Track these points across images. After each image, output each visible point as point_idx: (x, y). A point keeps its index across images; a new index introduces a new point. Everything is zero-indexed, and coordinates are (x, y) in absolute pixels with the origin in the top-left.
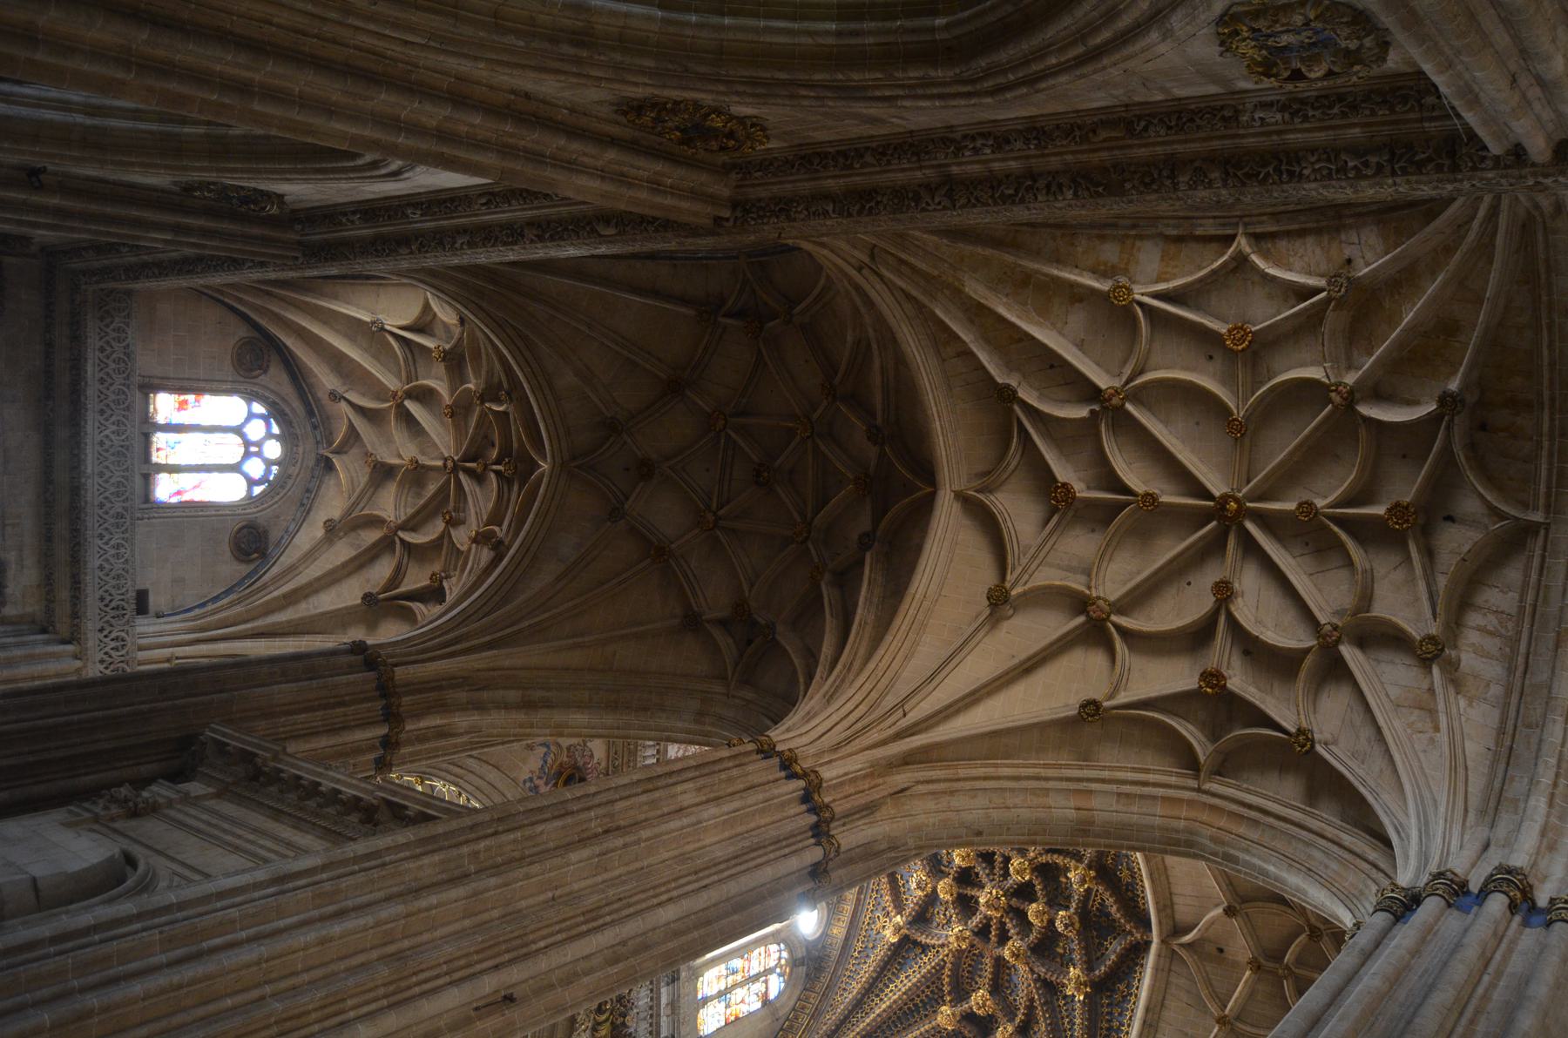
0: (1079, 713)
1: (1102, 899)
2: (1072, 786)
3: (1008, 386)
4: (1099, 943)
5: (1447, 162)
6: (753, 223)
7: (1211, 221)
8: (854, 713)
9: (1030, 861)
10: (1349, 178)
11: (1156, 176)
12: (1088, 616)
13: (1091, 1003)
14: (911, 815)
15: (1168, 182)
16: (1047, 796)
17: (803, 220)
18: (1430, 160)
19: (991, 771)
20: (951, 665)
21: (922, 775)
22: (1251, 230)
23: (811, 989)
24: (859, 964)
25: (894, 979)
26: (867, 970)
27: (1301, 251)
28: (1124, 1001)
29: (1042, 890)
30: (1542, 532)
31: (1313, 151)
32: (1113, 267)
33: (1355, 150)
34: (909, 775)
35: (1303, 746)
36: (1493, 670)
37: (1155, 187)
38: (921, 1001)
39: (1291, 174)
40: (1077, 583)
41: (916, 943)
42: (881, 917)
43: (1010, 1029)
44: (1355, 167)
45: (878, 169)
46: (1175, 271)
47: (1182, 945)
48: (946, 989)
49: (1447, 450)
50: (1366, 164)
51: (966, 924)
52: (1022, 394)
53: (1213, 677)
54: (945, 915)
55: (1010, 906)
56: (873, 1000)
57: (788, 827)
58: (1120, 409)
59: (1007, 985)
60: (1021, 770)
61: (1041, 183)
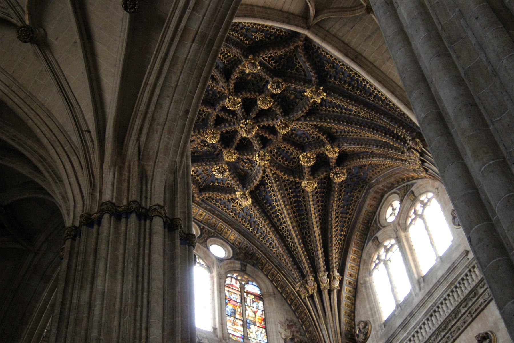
0: (130, 13)
1: (269, 58)
2: (177, 39)
4: (296, 70)
8: (75, 166)
9: (230, 94)
14: (158, 152)
19: (148, 88)
20: (66, 87)
21: (134, 136)
24: (258, 229)
25: (274, 210)
26: (264, 226)
28: (337, 69)
29: (251, 94)
34: (131, 143)
38: (294, 197)
41: (257, 187)
42: (234, 205)
43: (328, 147)
47: (315, 17)
48: (291, 179)
51: (256, 151)
55: (254, 118)
56: (283, 228)
57: (132, 234)
59: (302, 139)
60: (155, 68)
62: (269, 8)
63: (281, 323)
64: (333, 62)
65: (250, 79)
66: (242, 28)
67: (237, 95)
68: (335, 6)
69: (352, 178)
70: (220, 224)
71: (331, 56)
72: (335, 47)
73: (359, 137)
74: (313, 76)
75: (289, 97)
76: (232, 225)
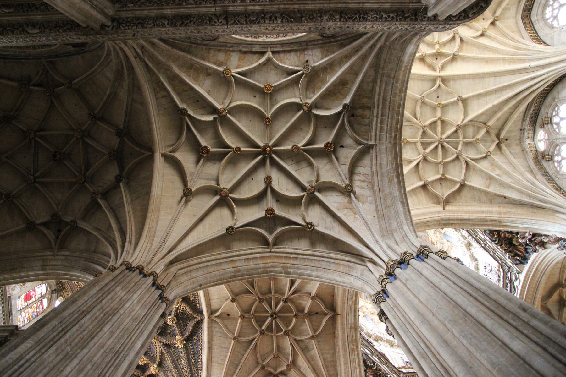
3: (184, 109)
5: (414, 18)
6: (123, 28)
7: (259, 46)
10: (382, 21)
11: (315, 16)
12: (221, 195)
13: (186, 347)
15: (319, 19)
16: (221, 265)
17: (150, 28)
18: (409, 16)
19: (199, 260)
22: (272, 49)
27: (289, 58)
30: (375, 147)
31: (372, 11)
32: (222, 62)
33: (385, 11)
35: (310, 228)
36: (367, 192)
37: (314, 20)
39: (364, 18)
40: (213, 183)
43: (156, 366)
44: (385, 17)
45: (194, 6)
46: (244, 64)
49: (343, 123)
50: (389, 16)
52: (190, 112)
53: (270, 211)
58: (225, 116)
59: (149, 350)
60: (209, 258)
61: (268, 16)
62: (209, 294)
64: (200, 340)
71: (201, 336)
72: (209, 335)
74: (187, 334)
75: (167, 330)
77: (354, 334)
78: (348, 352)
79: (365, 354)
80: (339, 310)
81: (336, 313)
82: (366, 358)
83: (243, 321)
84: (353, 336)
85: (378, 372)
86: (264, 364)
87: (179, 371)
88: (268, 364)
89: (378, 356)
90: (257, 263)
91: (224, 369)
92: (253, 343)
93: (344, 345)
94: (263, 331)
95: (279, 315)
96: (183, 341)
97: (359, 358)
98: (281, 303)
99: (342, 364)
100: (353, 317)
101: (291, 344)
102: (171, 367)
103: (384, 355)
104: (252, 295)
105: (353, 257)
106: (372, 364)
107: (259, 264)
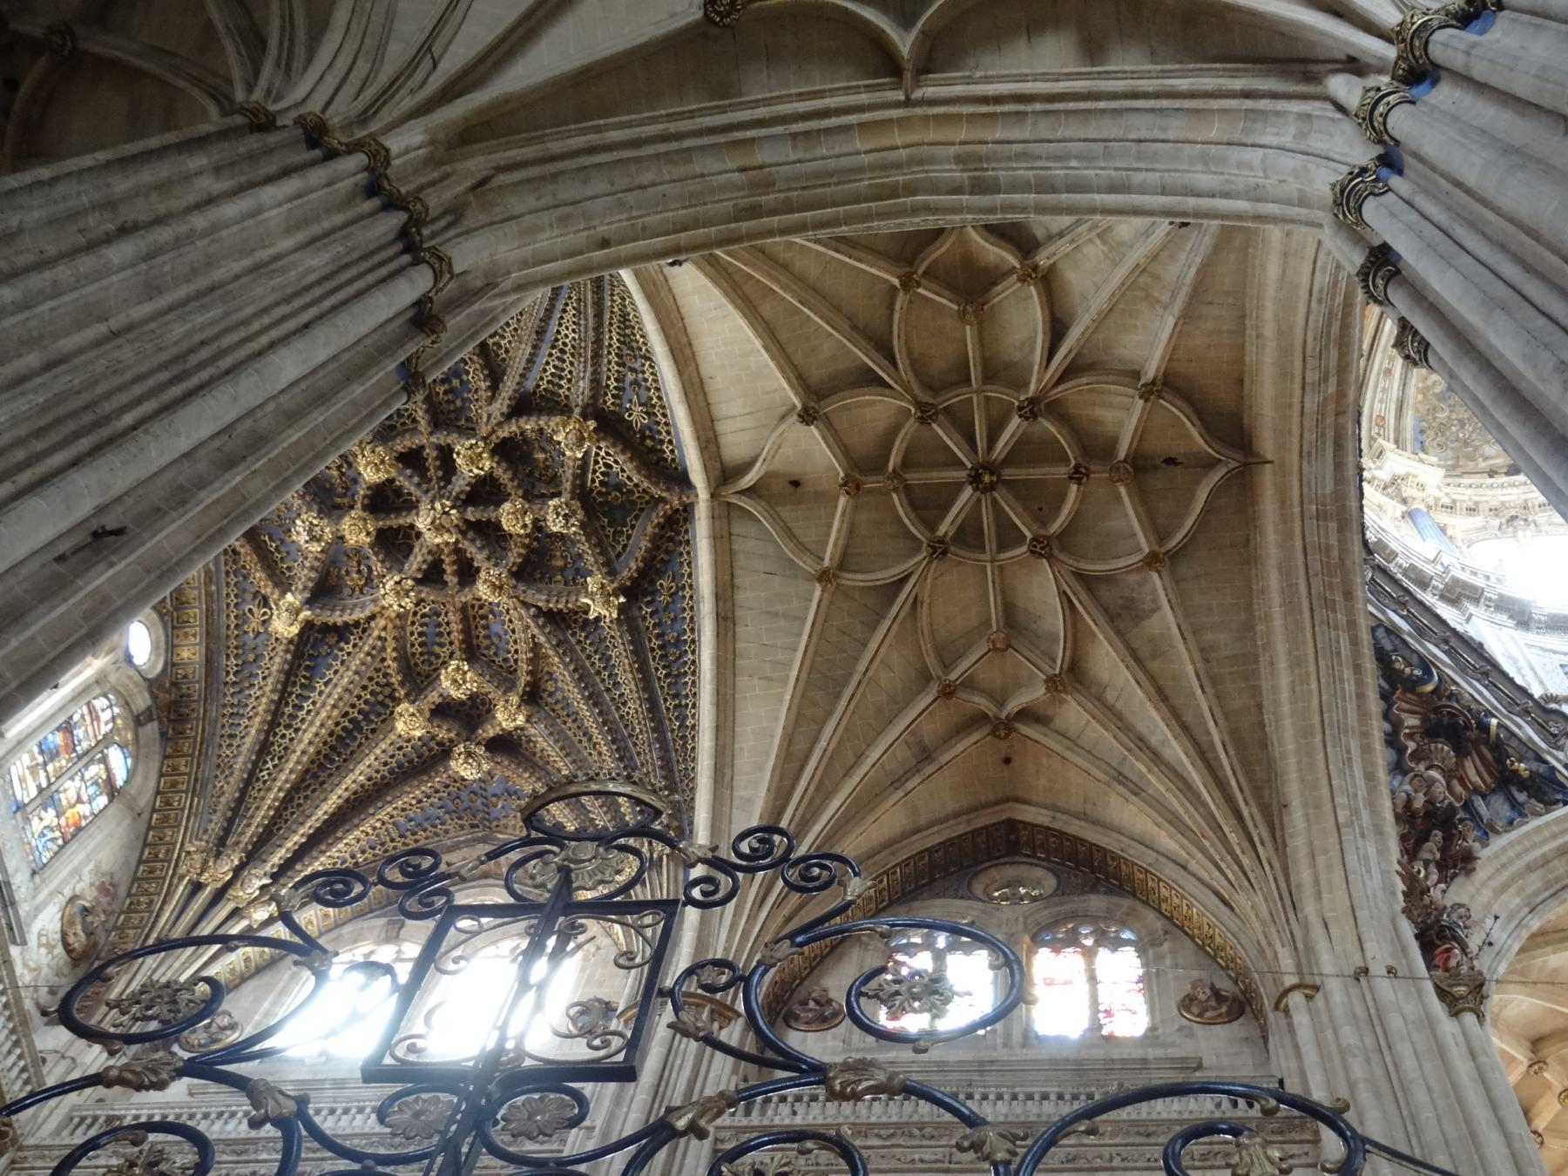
0: (706, 14)
1: (606, 465)
2: (721, 139)
8: (355, 72)
16: (690, 161)
19: (593, 138)
21: (501, 157)
23: (178, 753)
24: (241, 691)
25: (306, 693)
26: (262, 695)
28: (674, 602)
29: (512, 480)
41: (327, 629)
42: (255, 610)
43: (515, 699)
47: (742, 492)
54: (359, 572)
55: (466, 521)
56: (283, 736)
59: (486, 642)
62: (705, 394)
63: (98, 866)
64: (684, 588)
65: (536, 460)
66: (633, 370)
67: (493, 452)
68: (785, 515)
69: (475, 794)
70: (196, 613)
71: (690, 575)
72: (717, 565)
73: (576, 740)
74: (630, 567)
75: (552, 557)
76: (212, 637)
77: (1333, 541)
78: (1307, 614)
79: (1388, 631)
80: (1267, 444)
81: (1258, 455)
82: (1388, 646)
83: (856, 508)
84: (1328, 548)
85: (1444, 701)
86: (953, 676)
87: (609, 713)
88: (969, 684)
89: (1446, 642)
90: (846, 149)
91: (788, 697)
92: (903, 596)
93: (1289, 590)
94: (941, 541)
95: (1009, 473)
96: (616, 594)
97: (1355, 642)
98: (1016, 421)
99: (1282, 663)
100: (1330, 468)
101: (1063, 594)
102: (574, 696)
103: (1481, 645)
104: (887, 391)
105: (1267, 74)
106: (1418, 672)
107: (858, 153)
